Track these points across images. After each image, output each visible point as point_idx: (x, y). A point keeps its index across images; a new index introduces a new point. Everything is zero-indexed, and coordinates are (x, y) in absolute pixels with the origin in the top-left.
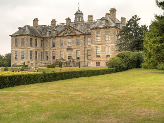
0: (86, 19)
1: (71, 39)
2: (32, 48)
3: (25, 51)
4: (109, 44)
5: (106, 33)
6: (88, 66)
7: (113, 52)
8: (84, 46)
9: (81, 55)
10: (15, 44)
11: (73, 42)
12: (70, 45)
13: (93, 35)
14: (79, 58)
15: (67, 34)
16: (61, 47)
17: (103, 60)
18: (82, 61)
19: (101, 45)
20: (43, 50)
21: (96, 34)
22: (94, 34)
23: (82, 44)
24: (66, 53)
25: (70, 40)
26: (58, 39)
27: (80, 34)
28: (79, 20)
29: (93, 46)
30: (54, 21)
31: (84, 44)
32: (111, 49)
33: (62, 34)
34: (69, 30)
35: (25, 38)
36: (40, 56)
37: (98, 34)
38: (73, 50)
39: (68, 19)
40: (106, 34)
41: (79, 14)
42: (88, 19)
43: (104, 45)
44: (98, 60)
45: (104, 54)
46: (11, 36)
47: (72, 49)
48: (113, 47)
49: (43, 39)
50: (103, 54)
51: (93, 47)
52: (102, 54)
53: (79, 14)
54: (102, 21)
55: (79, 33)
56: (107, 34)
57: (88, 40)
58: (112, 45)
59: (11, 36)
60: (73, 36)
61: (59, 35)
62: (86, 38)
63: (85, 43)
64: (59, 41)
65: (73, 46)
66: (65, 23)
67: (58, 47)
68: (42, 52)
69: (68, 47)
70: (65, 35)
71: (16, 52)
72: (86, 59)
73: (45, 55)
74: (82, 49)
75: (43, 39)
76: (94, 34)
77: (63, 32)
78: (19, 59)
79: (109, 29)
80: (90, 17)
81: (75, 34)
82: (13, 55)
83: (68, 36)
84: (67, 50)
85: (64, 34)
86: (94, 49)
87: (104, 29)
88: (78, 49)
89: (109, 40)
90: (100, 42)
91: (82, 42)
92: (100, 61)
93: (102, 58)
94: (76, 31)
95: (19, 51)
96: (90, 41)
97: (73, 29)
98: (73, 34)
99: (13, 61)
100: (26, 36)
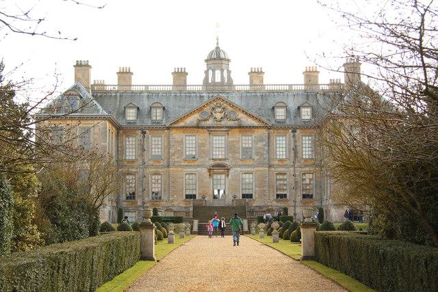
0: (241, 79)
1: (223, 138)
8: (266, 161)
9: (257, 189)
11: (231, 148)
12: (219, 154)
14: (251, 195)
15: (210, 122)
23: (262, 155)
24: (207, 179)
25: (219, 141)
26: (176, 135)
27: (255, 123)
31: (266, 156)
33: (191, 120)
38: (231, 171)
39: (180, 75)
42: (251, 81)
47: (228, 170)
60: (231, 127)
61: (182, 124)
67: (176, 160)
69: (212, 163)
70: (204, 124)
74: (261, 169)
83: (213, 127)
84: (209, 170)
85: (199, 121)
88: (249, 169)
94: (241, 115)
96: (223, 146)
97: (230, 108)
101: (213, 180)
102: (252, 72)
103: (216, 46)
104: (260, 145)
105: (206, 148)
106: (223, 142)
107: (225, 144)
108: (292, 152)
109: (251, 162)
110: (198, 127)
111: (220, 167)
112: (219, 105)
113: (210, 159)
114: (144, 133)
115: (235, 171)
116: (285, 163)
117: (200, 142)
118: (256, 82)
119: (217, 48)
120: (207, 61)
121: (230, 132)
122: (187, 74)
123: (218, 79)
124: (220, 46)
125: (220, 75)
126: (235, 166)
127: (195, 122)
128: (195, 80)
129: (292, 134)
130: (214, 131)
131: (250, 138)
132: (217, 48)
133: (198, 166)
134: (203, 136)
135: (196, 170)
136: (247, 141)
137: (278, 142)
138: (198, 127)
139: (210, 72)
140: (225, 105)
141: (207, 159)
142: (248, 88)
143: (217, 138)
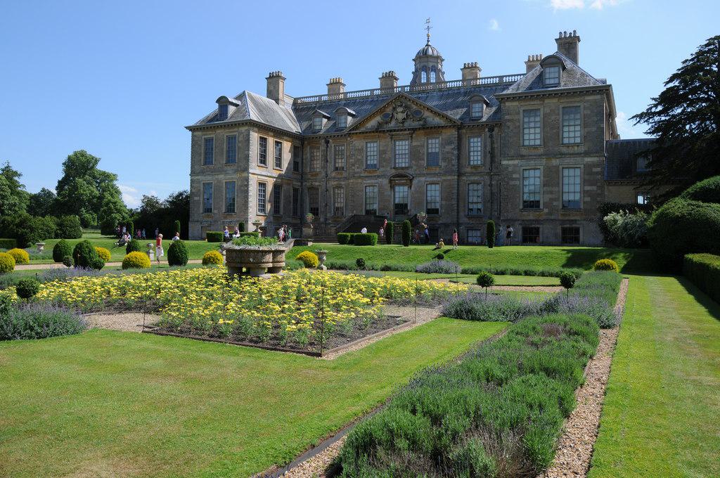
2: (263, 173)
3: (238, 183)
4: (579, 154)
5: (563, 114)
6: (470, 240)
7: (594, 188)
9: (444, 203)
10: (205, 158)
11: (414, 154)
12: (402, 162)
13: (509, 120)
15: (392, 124)
16: (370, 172)
17: (553, 217)
18: (449, 221)
19: (544, 161)
20: (302, 183)
21: (524, 116)
22: (516, 117)
25: (403, 146)
26: (358, 143)
28: (428, 79)
29: (511, 162)
30: (335, 85)
31: (455, 162)
32: (587, 177)
33: (372, 123)
34: (400, 109)
35: (241, 136)
36: (290, 203)
37: (532, 119)
38: (415, 182)
39: (389, 78)
40: (563, 120)
41: (426, 61)
43: (555, 162)
44: (531, 217)
45: (554, 196)
46: (191, 130)
47: (411, 180)
48: (595, 170)
49: (303, 144)
50: (550, 196)
51: (510, 169)
52: (548, 197)
53: (426, 61)
54: (547, 70)
55: (437, 121)
56: (569, 120)
57: (469, 147)
58: (588, 160)
59: (190, 128)
60: (414, 130)
61: (362, 129)
62: (465, 141)
63: (459, 158)
64: (360, 150)
65: (415, 168)
68: (295, 190)
69: (393, 171)
70: (386, 127)
71: (207, 186)
72: (462, 214)
73: (308, 200)
74: (449, 178)
75: (303, 144)
76: (516, 117)
77: (378, 119)
78: (216, 211)
79: (578, 99)
80: (470, 69)
81: (421, 122)
82: (196, 198)
83: (395, 130)
84: (391, 181)
85: (380, 124)
86: (514, 176)
87: (555, 100)
89: (578, 140)
90: (541, 151)
91: (448, 153)
92: (537, 221)
93: (546, 210)
94: (427, 114)
95: (219, 182)
97: (415, 107)
98: (416, 124)
99: (196, 219)
100: (243, 129)
102: (465, 67)
104: (448, 148)
105: (389, 155)
108: (489, 156)
109: (438, 170)
110: (378, 130)
111: (401, 177)
113: (391, 168)
114: (327, 142)
115: (419, 181)
116: (479, 170)
117: (381, 149)
121: (414, 135)
124: (430, 43)
125: (425, 76)
126: (420, 175)
128: (404, 79)
129: (488, 134)
131: (437, 141)
133: (379, 177)
134: (385, 141)
136: (434, 145)
137: (472, 144)
138: (378, 130)
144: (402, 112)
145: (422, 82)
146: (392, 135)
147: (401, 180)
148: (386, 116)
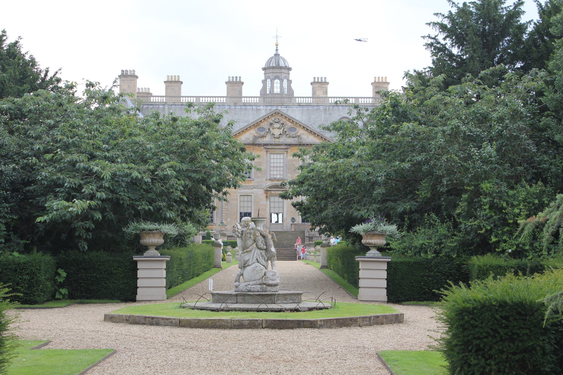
1: (282, 156)
15: (268, 139)
34: (277, 125)
42: (314, 92)
60: (290, 145)
66: (226, 95)
69: (269, 183)
70: (261, 141)
81: (296, 139)
83: (271, 145)
84: (266, 191)
85: (256, 138)
94: (301, 132)
97: (289, 124)
101: (270, 202)
103: (274, 52)
106: (282, 161)
107: (283, 163)
112: (277, 121)
113: (266, 180)
118: (320, 93)
119: (277, 55)
120: (264, 69)
121: (289, 150)
122: (243, 83)
123: (277, 90)
124: (279, 52)
125: (279, 85)
127: (251, 139)
130: (272, 149)
132: (277, 55)
135: (251, 191)
139: (269, 81)
140: (284, 120)
141: (264, 179)
142: (310, 101)
143: (275, 156)
144: (279, 128)
145: (275, 92)
146: (268, 149)
147: (277, 190)
148: (263, 129)
